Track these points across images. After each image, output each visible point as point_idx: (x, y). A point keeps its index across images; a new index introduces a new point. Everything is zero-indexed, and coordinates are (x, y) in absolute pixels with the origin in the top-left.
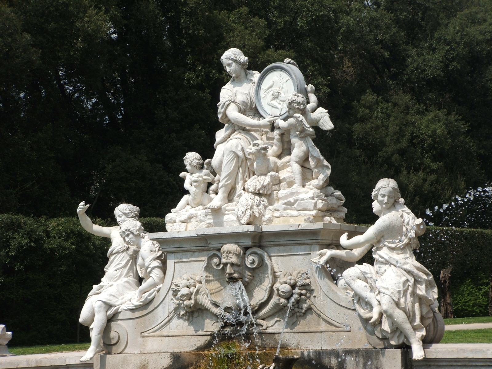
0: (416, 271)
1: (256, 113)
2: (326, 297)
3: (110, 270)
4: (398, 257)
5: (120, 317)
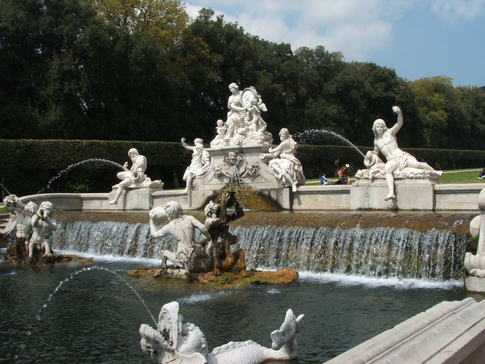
0: (294, 161)
1: (241, 106)
2: (264, 169)
3: (193, 161)
4: (288, 156)
5: (196, 178)
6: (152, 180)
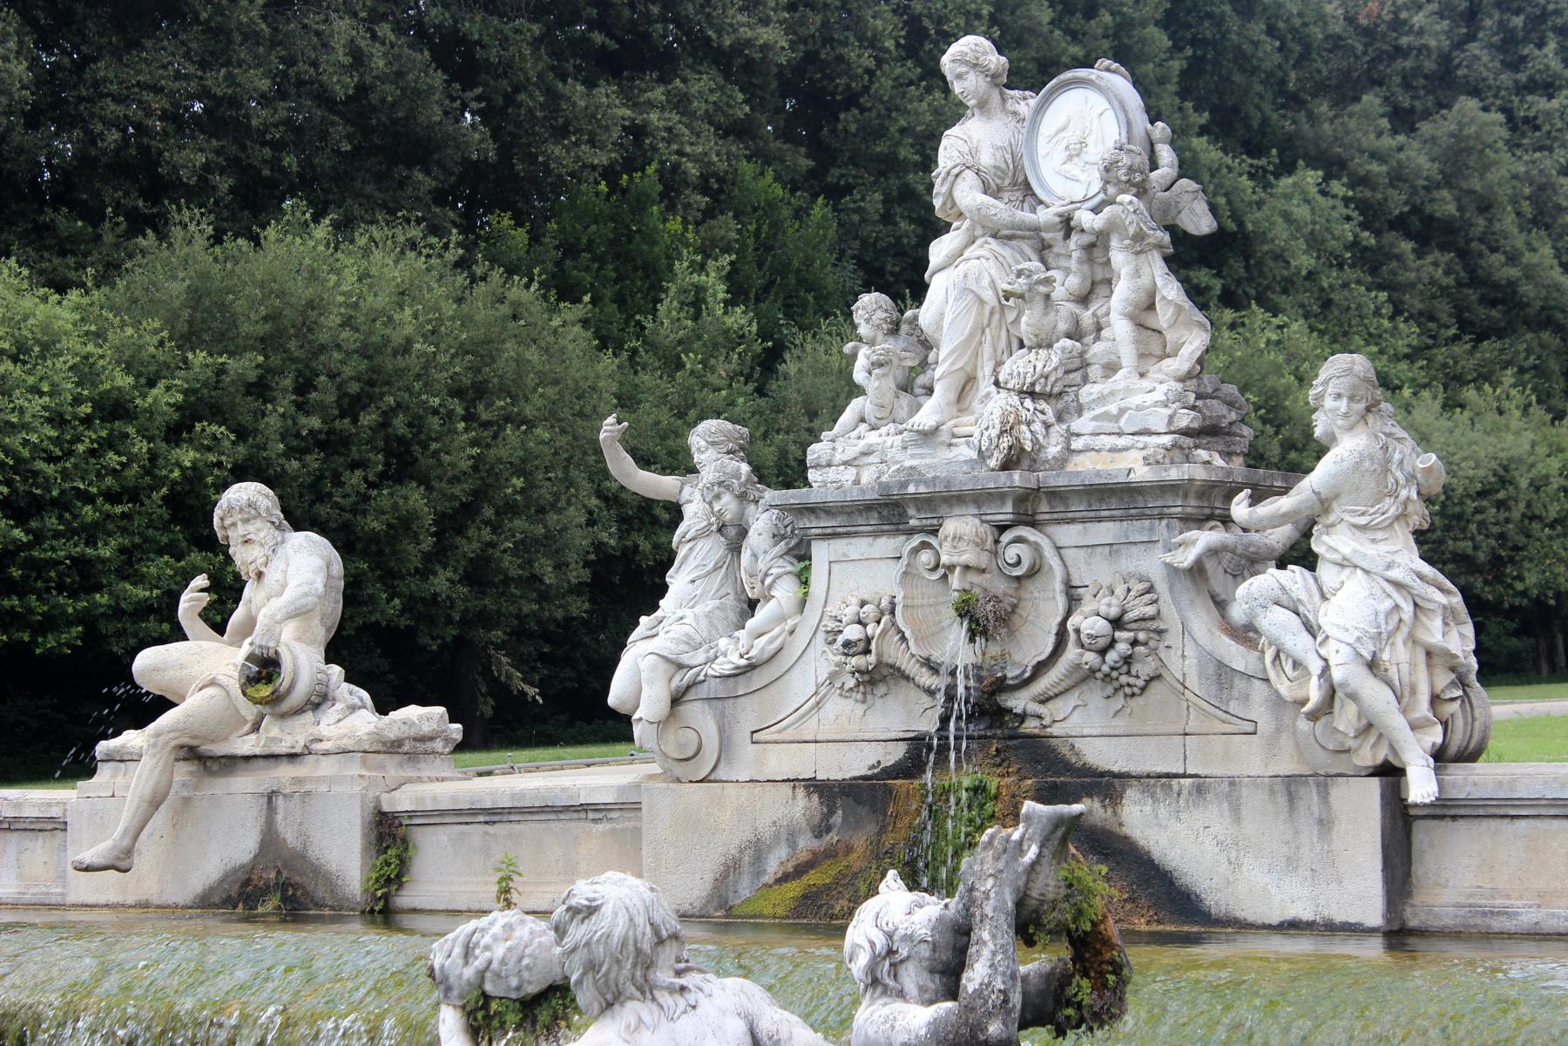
0: (1418, 586)
1: (1026, 191)
3: (677, 580)
4: (1373, 551)
6: (382, 708)
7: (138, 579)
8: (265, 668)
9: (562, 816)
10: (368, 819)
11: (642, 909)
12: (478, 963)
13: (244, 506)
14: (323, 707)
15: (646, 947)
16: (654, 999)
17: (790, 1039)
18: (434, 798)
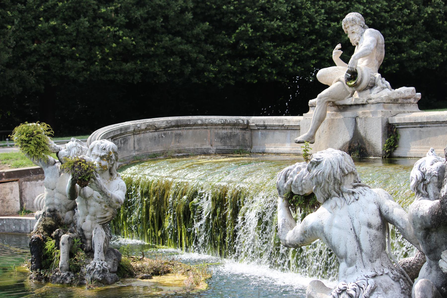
7: (416, 49)
8: (353, 75)
9: (442, 125)
10: (384, 126)
11: (336, 163)
12: (288, 181)
13: (352, 21)
14: (373, 88)
15: (338, 177)
16: (343, 196)
17: (393, 212)
18: (404, 119)
